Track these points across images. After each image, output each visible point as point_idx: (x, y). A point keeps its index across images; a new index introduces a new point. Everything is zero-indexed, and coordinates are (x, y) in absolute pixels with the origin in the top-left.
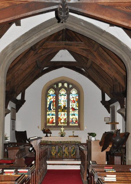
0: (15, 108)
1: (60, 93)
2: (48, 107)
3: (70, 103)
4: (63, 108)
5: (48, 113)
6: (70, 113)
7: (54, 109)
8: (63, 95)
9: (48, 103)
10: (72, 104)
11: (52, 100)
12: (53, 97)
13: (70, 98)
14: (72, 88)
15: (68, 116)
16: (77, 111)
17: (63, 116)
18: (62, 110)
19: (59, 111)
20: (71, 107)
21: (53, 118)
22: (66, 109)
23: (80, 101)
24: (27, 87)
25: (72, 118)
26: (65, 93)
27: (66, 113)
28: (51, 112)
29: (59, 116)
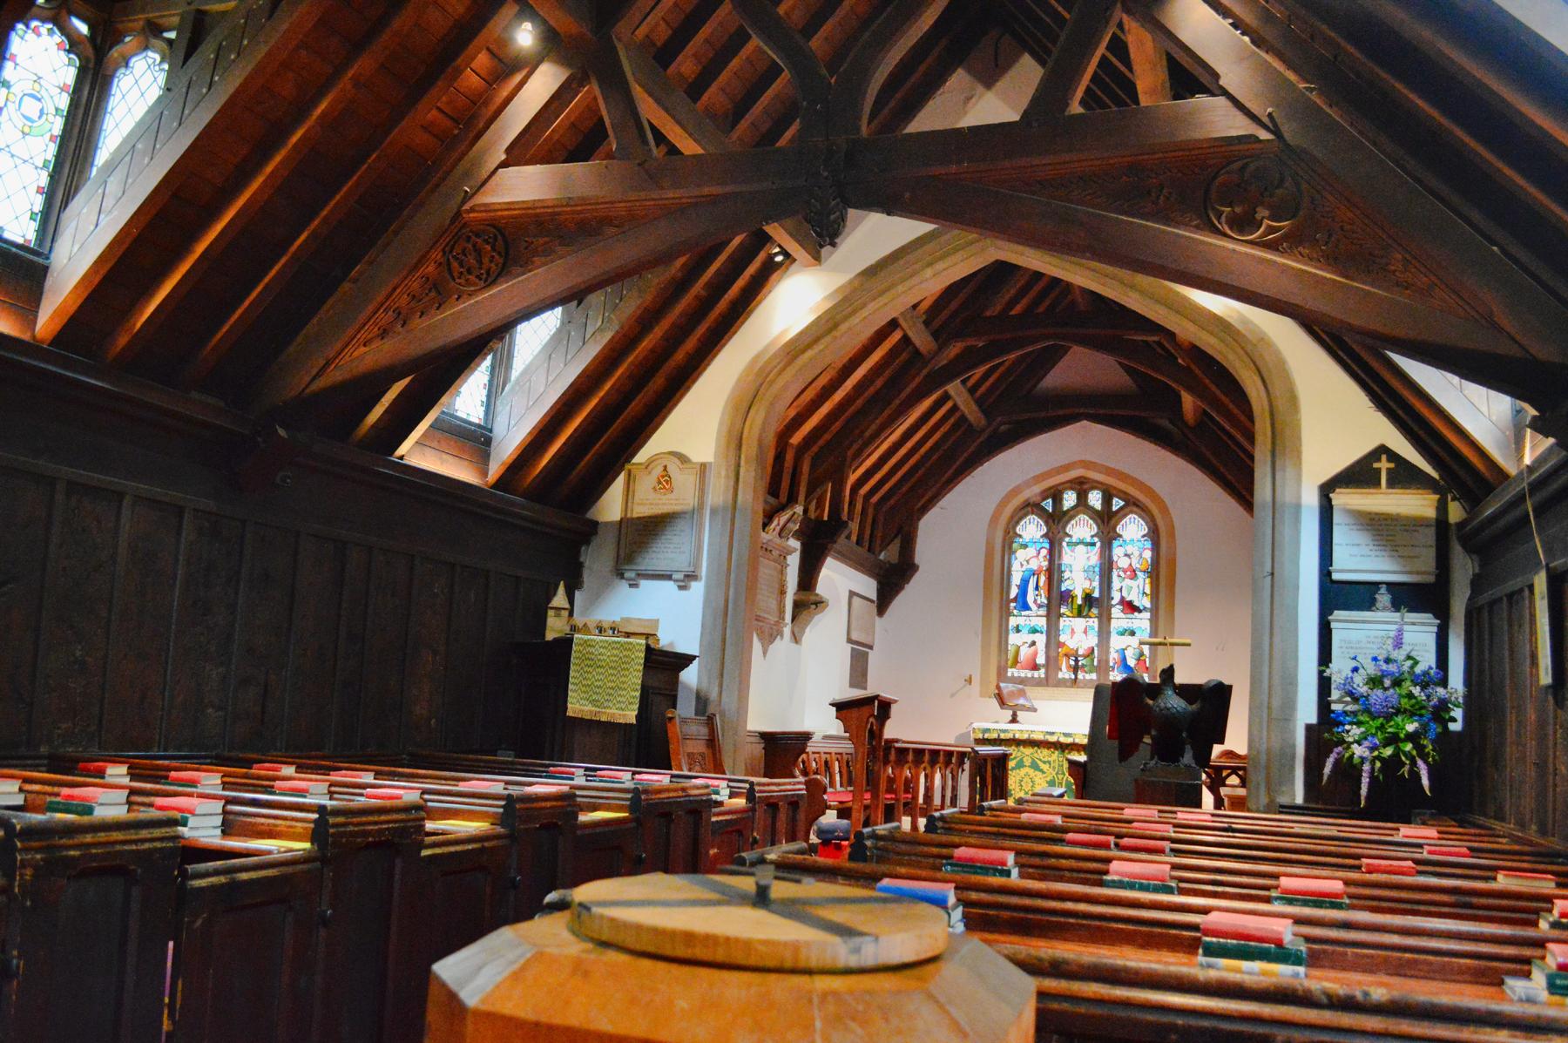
0: (874, 596)
2: (1012, 595)
4: (1079, 602)
5: (1013, 621)
6: (1114, 623)
7: (1040, 606)
8: (1081, 542)
9: (1016, 579)
11: (1034, 565)
15: (1104, 634)
16: (1147, 615)
17: (1079, 635)
19: (1061, 615)
20: (1116, 597)
21: (1034, 643)
22: (1094, 604)
23: (1161, 573)
24: (925, 509)
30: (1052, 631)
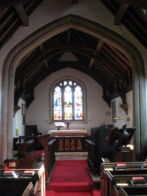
0: (26, 105)
5: (55, 109)
14: (76, 86)
15: (73, 110)
16: (82, 106)
24: (36, 86)
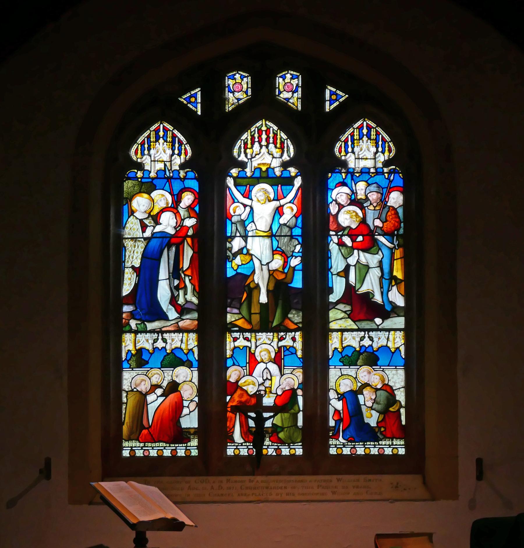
1: (242, 165)
2: (127, 289)
3: (333, 247)
4: (263, 298)
6: (334, 342)
7: (182, 310)
9: (134, 256)
10: (352, 261)
11: (168, 223)
12: (177, 199)
13: (333, 209)
14: (344, 117)
16: (399, 322)
18: (256, 319)
20: (338, 287)
21: (173, 387)
25: (345, 386)
26: (285, 165)
27: (299, 345)
28: (160, 332)
29: (232, 374)
30: (211, 363)
